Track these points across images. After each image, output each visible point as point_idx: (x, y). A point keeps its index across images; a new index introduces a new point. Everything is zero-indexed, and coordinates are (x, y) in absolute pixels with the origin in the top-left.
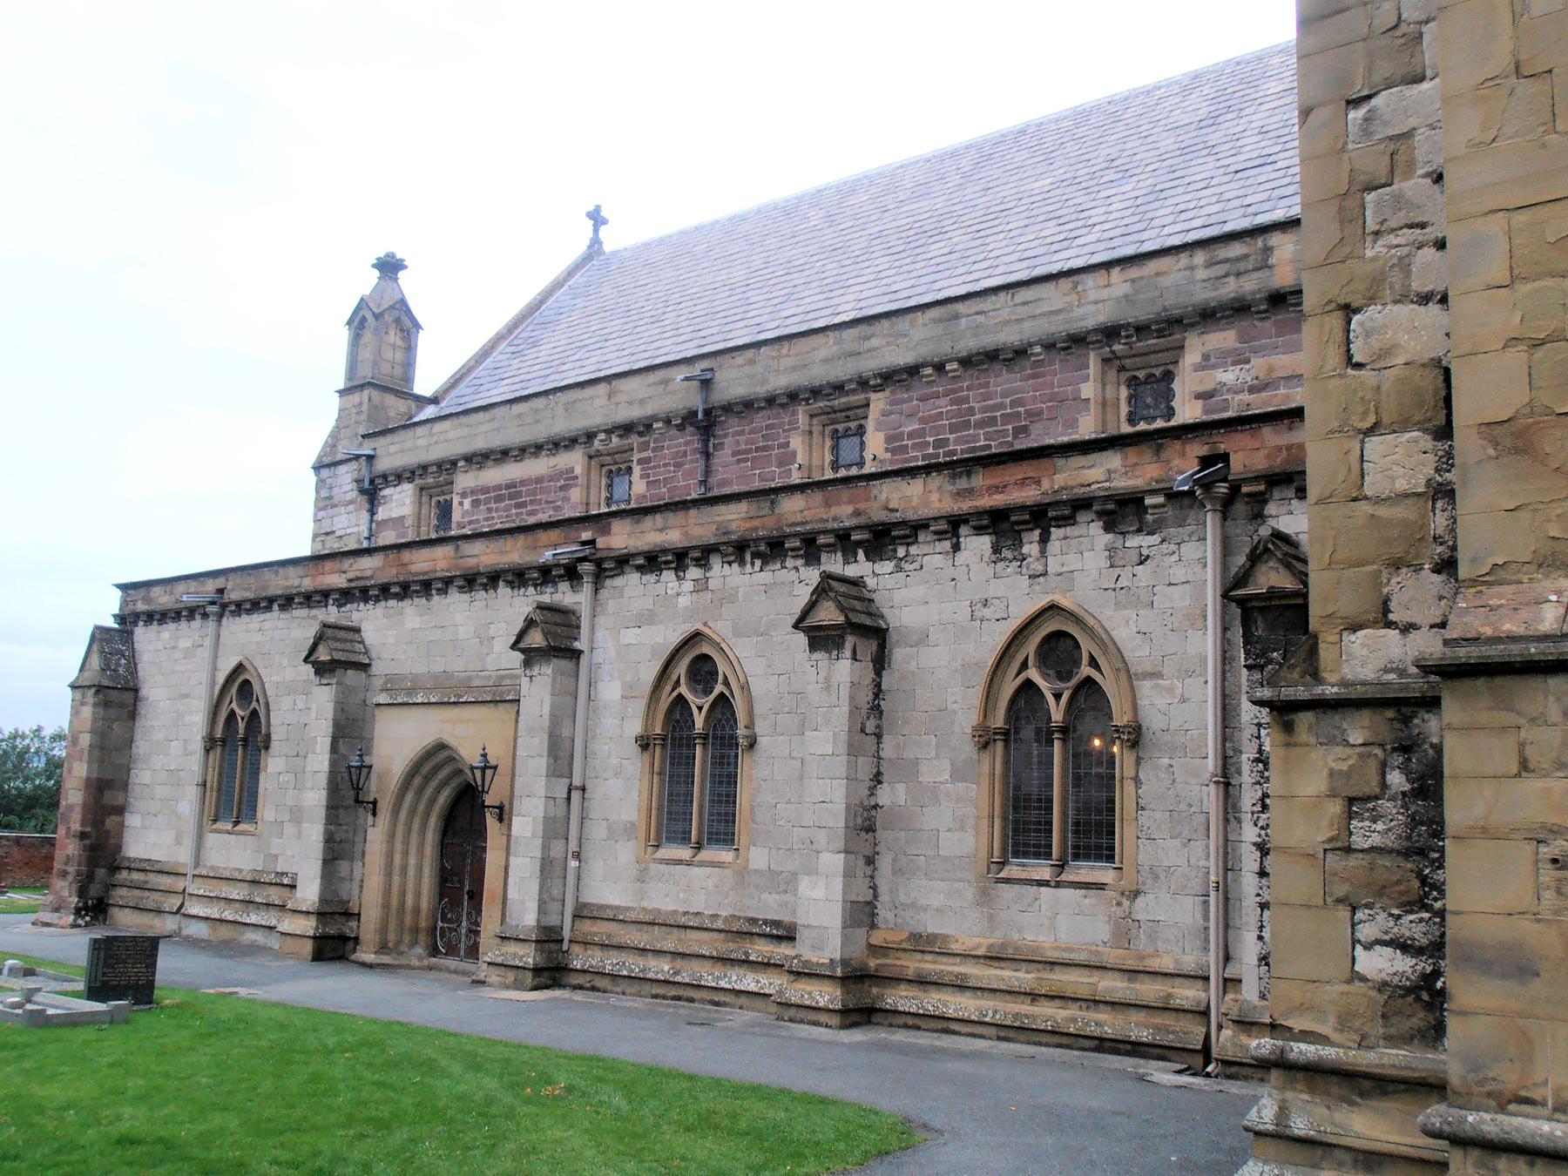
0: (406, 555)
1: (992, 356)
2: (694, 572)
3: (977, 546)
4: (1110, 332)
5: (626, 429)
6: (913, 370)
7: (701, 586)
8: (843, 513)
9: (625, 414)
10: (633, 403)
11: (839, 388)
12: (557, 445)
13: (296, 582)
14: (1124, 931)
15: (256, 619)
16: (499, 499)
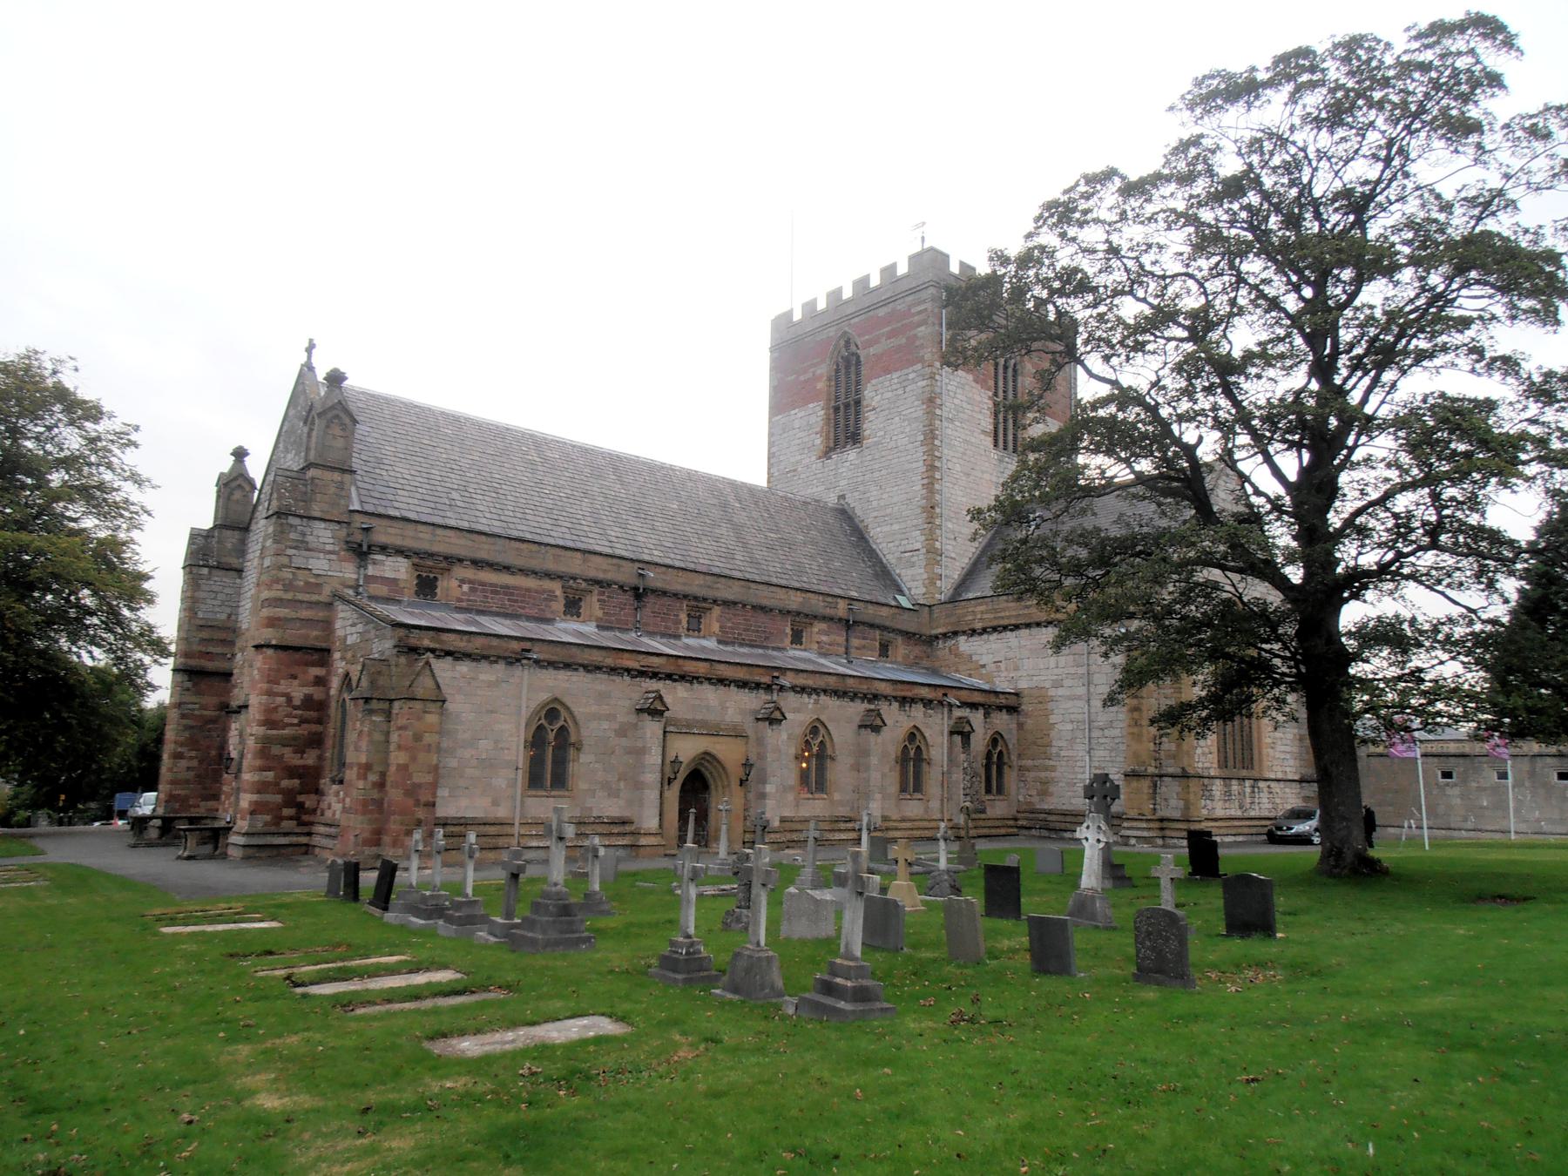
0: (680, 662)
1: (763, 609)
2: (814, 696)
3: (896, 705)
4: (798, 614)
6: (735, 603)
7: (816, 702)
8: (864, 688)
9: (592, 574)
10: (596, 569)
11: (705, 600)
12: (548, 575)
13: (600, 659)
14: (927, 809)
16: (496, 592)
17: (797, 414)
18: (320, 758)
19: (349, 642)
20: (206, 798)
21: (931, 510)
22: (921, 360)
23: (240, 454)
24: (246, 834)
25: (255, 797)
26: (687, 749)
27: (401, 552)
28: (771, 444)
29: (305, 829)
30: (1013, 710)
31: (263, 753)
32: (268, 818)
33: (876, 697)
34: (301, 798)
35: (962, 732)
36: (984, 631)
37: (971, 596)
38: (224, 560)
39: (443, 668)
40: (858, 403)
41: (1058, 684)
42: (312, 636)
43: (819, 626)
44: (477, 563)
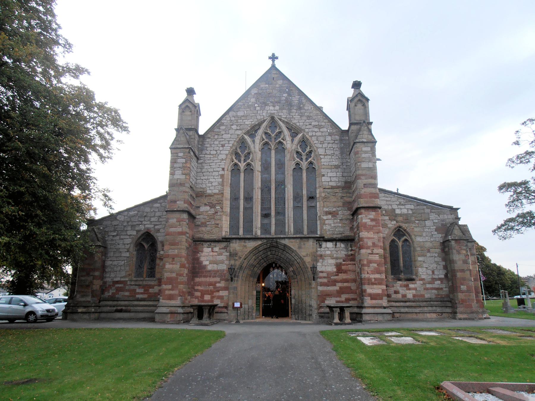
19: (397, 212)
23: (191, 92)
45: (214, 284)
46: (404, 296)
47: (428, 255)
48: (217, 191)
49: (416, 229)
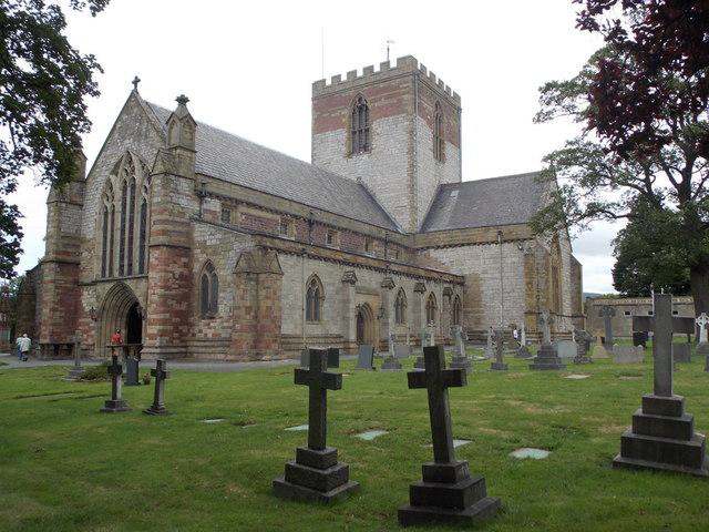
1: (356, 233)
5: (296, 217)
6: (346, 230)
9: (293, 212)
10: (295, 209)
12: (277, 212)
15: (317, 262)
17: (331, 135)
18: (189, 306)
20: (69, 333)
21: (412, 187)
22: (406, 111)
24: (160, 347)
25: (161, 327)
26: (362, 299)
27: (218, 197)
28: (313, 149)
29: (183, 344)
30: (462, 284)
31: (164, 304)
32: (167, 338)
33: (418, 277)
34: (180, 328)
35: (447, 293)
36: (445, 246)
37: (432, 230)
38: (74, 199)
39: (282, 258)
40: (367, 130)
41: (485, 272)
42: (180, 240)
43: (376, 242)
44: (249, 204)
45: (88, 324)
46: (206, 335)
47: (229, 290)
48: (91, 237)
49: (222, 262)
